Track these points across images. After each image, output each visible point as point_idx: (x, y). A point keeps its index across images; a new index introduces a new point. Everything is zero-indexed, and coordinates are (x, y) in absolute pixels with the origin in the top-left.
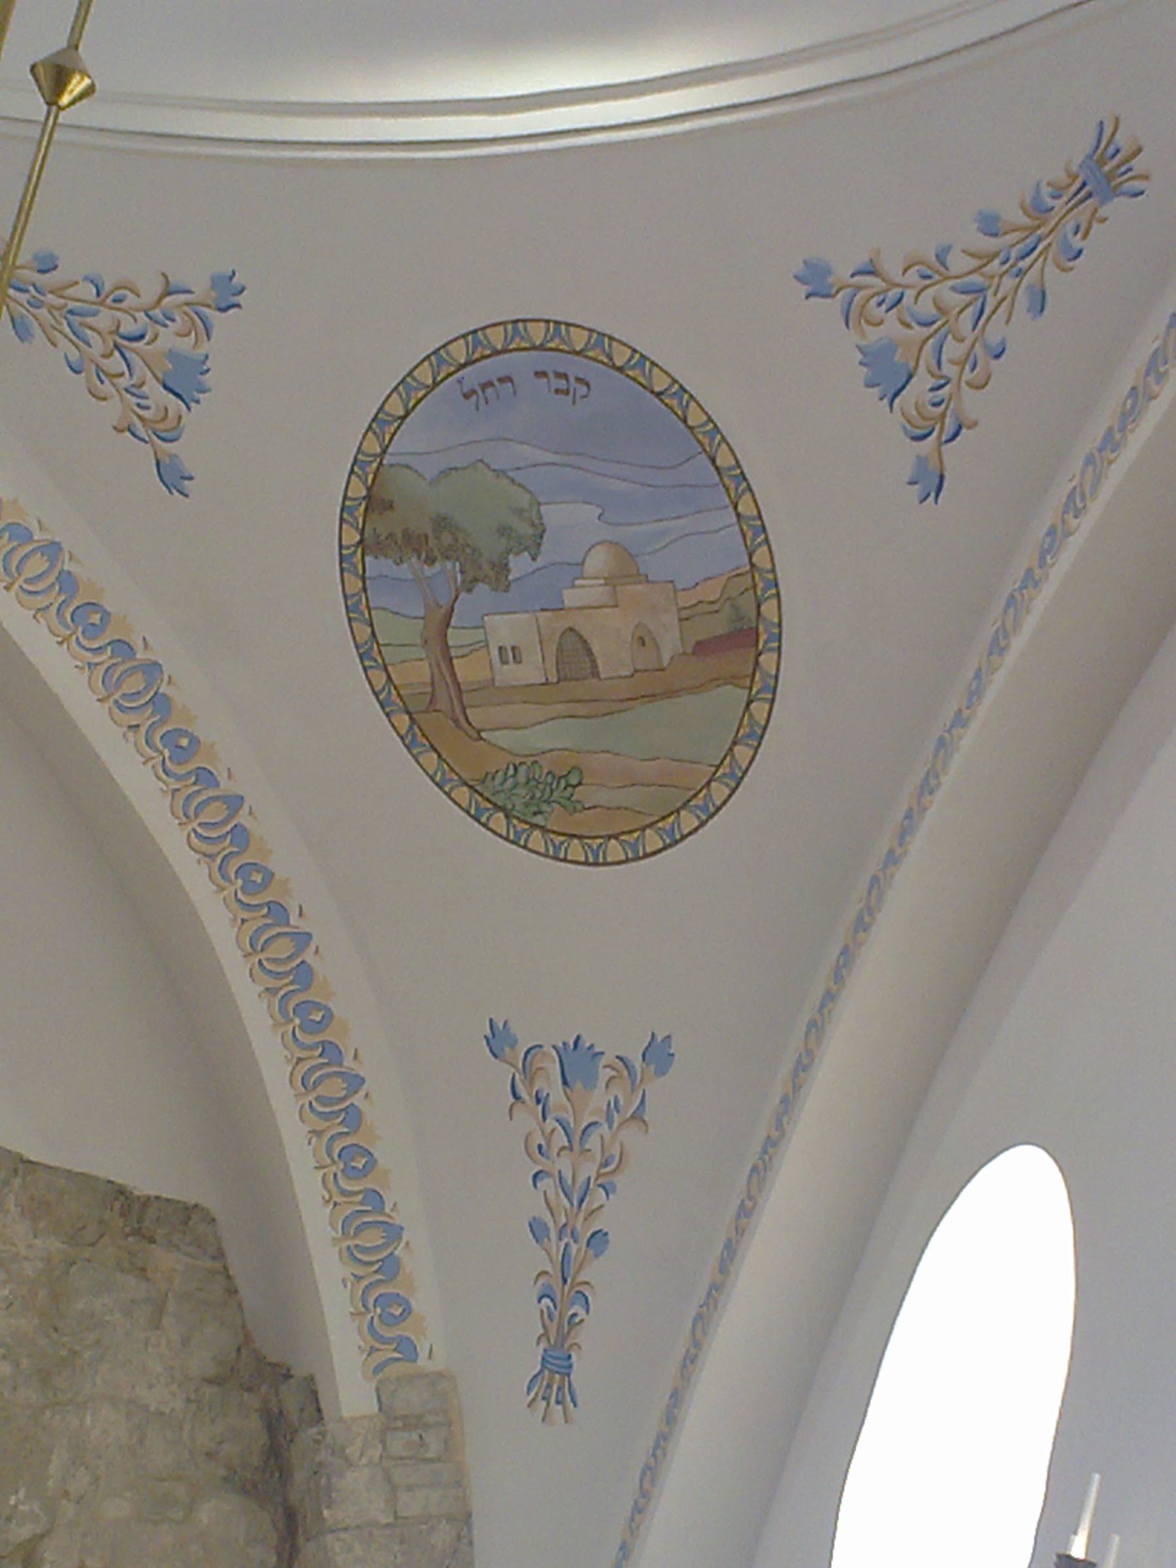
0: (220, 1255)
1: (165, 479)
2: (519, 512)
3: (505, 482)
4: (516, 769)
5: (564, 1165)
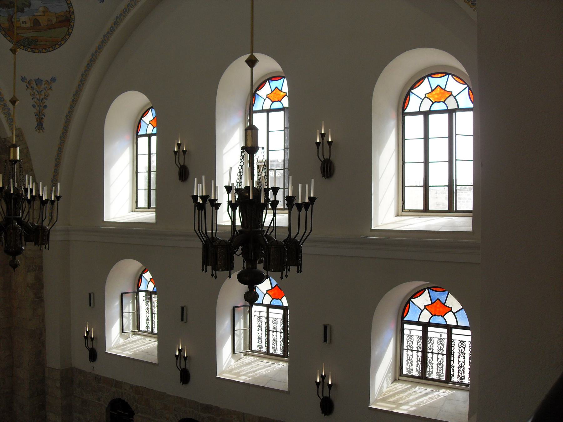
5: (38, 96)
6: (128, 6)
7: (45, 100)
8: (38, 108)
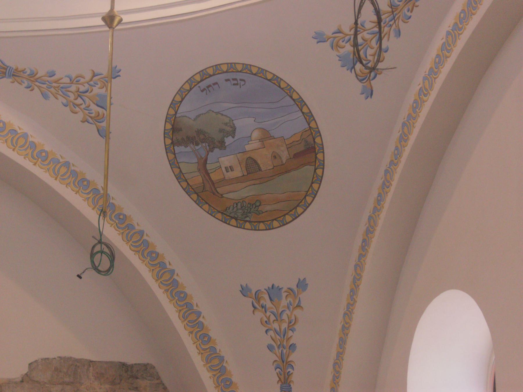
0: (159, 378)
1: (101, 134)
2: (226, 124)
3: (220, 115)
4: (237, 204)
5: (276, 326)
6: (419, 94)
7: (290, 333)
8: (278, 352)
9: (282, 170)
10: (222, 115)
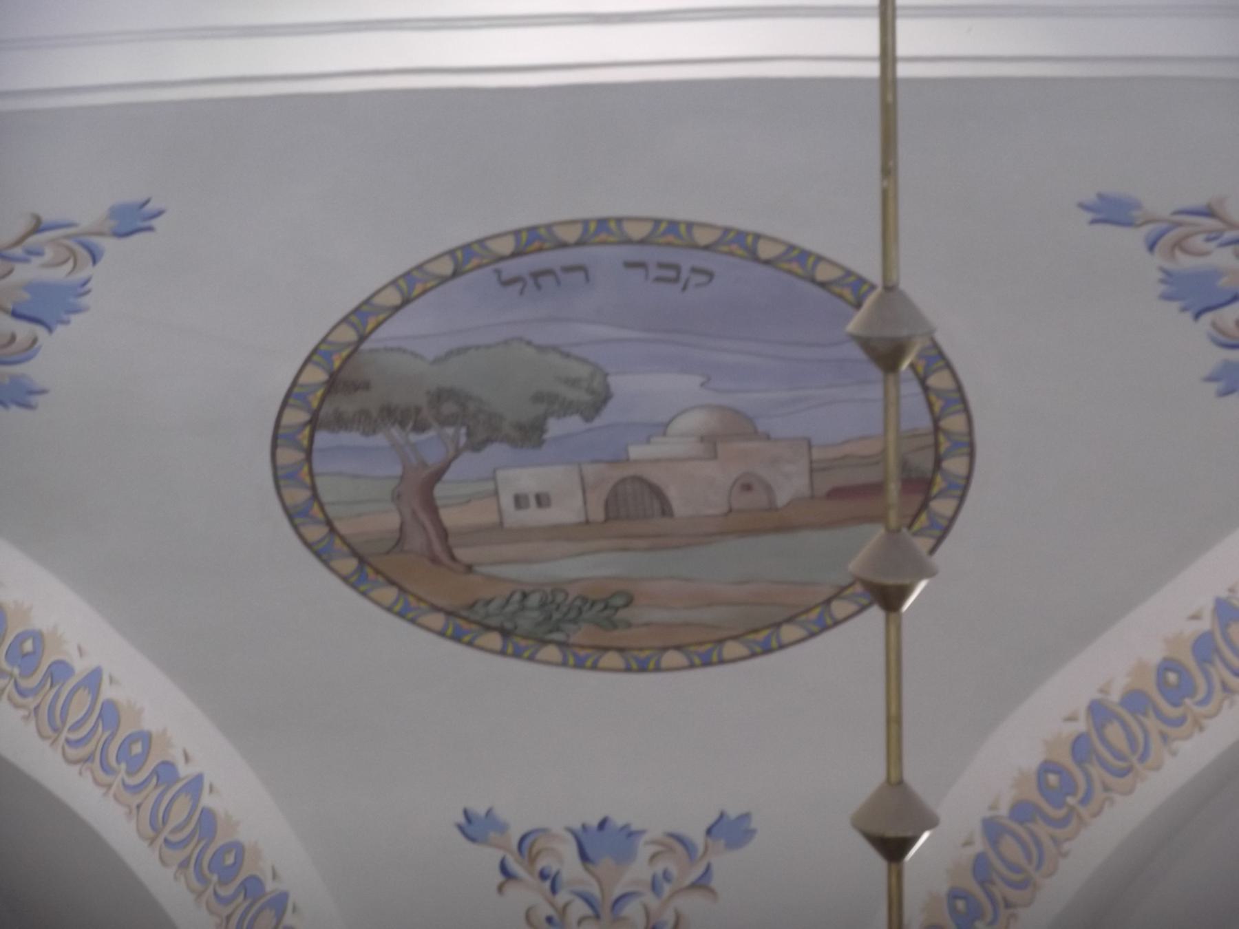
2: (573, 383)
9: (755, 518)
10: (567, 355)
